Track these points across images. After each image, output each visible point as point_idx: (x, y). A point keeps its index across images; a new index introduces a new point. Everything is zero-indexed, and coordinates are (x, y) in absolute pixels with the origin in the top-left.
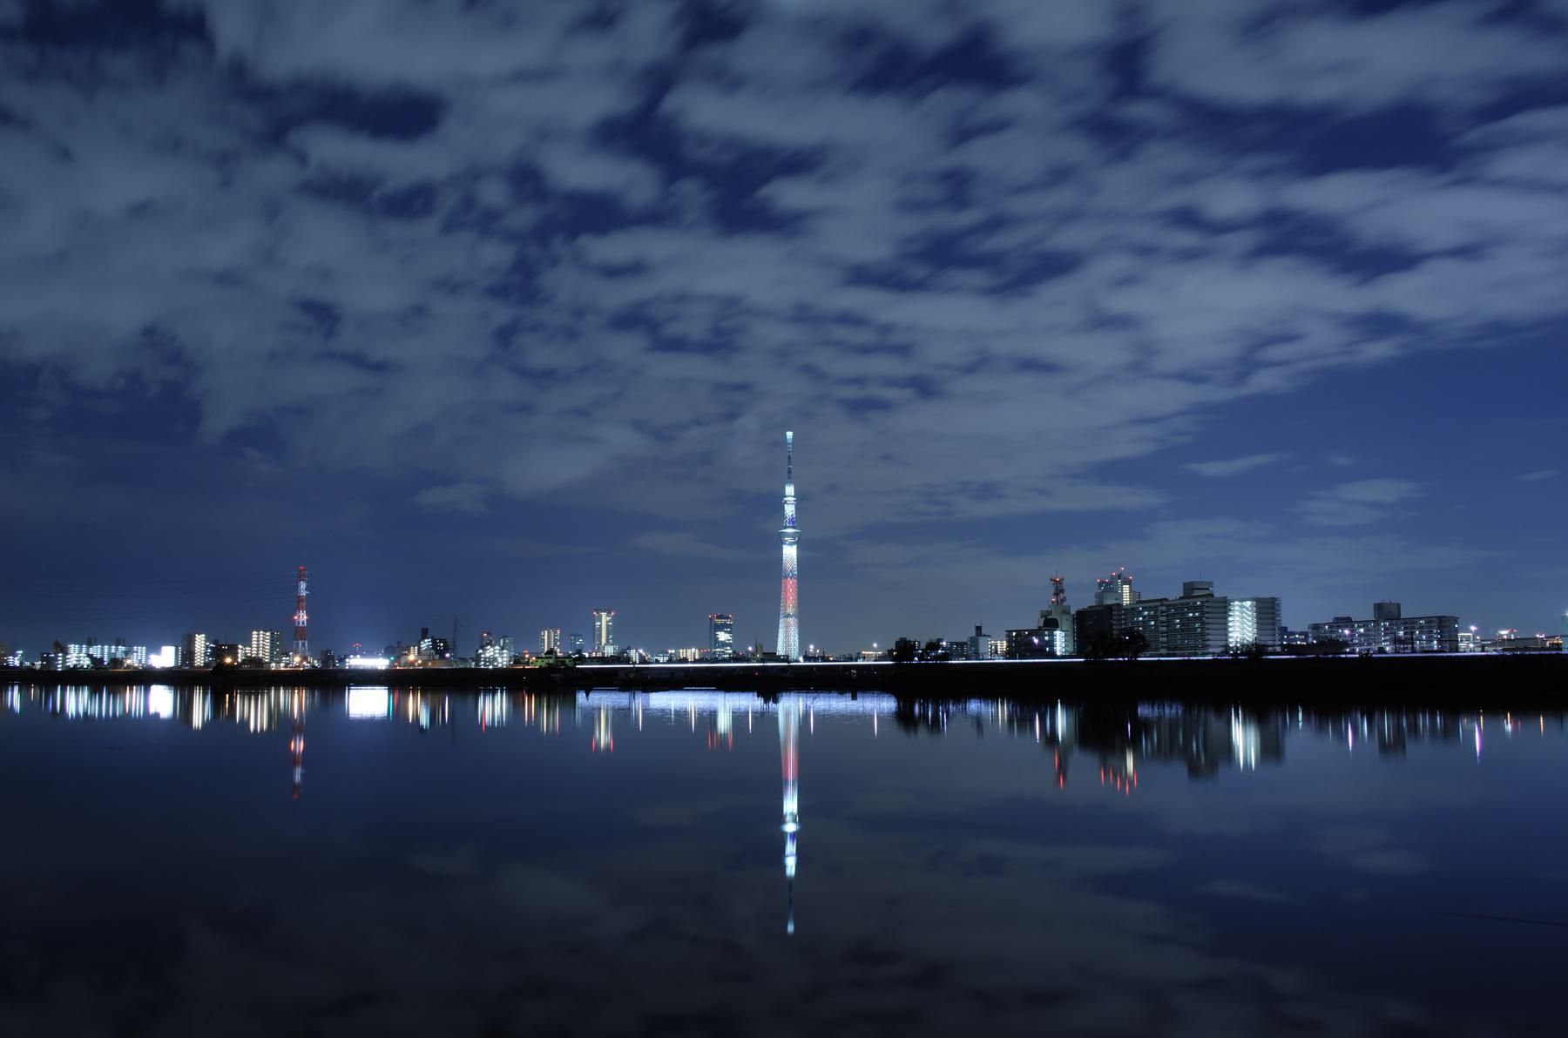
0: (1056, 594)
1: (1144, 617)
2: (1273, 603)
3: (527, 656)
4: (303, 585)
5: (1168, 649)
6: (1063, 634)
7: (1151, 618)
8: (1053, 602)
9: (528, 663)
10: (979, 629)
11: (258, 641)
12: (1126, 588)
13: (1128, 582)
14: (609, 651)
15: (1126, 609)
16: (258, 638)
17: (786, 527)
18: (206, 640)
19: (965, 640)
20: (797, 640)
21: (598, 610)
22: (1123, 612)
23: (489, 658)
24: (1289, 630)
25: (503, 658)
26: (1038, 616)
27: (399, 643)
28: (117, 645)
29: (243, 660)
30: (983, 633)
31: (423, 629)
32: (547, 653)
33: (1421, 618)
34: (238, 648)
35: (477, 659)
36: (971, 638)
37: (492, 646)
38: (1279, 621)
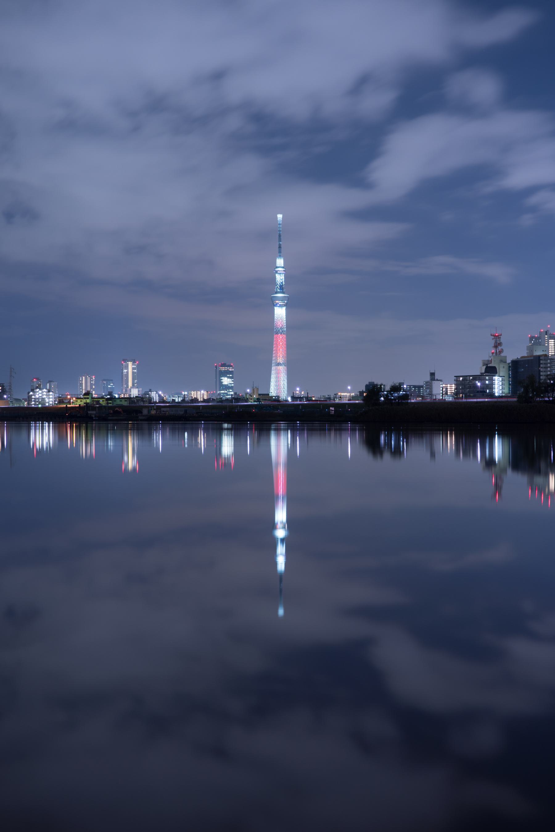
0: (496, 347)
3: (69, 397)
8: (493, 353)
9: (69, 403)
10: (432, 374)
14: (135, 393)
15: (551, 359)
17: (277, 293)
21: (125, 360)
22: (549, 361)
23: (38, 399)
25: (49, 398)
26: (481, 364)
30: (436, 378)
32: (85, 394)
35: (29, 399)
37: (40, 389)
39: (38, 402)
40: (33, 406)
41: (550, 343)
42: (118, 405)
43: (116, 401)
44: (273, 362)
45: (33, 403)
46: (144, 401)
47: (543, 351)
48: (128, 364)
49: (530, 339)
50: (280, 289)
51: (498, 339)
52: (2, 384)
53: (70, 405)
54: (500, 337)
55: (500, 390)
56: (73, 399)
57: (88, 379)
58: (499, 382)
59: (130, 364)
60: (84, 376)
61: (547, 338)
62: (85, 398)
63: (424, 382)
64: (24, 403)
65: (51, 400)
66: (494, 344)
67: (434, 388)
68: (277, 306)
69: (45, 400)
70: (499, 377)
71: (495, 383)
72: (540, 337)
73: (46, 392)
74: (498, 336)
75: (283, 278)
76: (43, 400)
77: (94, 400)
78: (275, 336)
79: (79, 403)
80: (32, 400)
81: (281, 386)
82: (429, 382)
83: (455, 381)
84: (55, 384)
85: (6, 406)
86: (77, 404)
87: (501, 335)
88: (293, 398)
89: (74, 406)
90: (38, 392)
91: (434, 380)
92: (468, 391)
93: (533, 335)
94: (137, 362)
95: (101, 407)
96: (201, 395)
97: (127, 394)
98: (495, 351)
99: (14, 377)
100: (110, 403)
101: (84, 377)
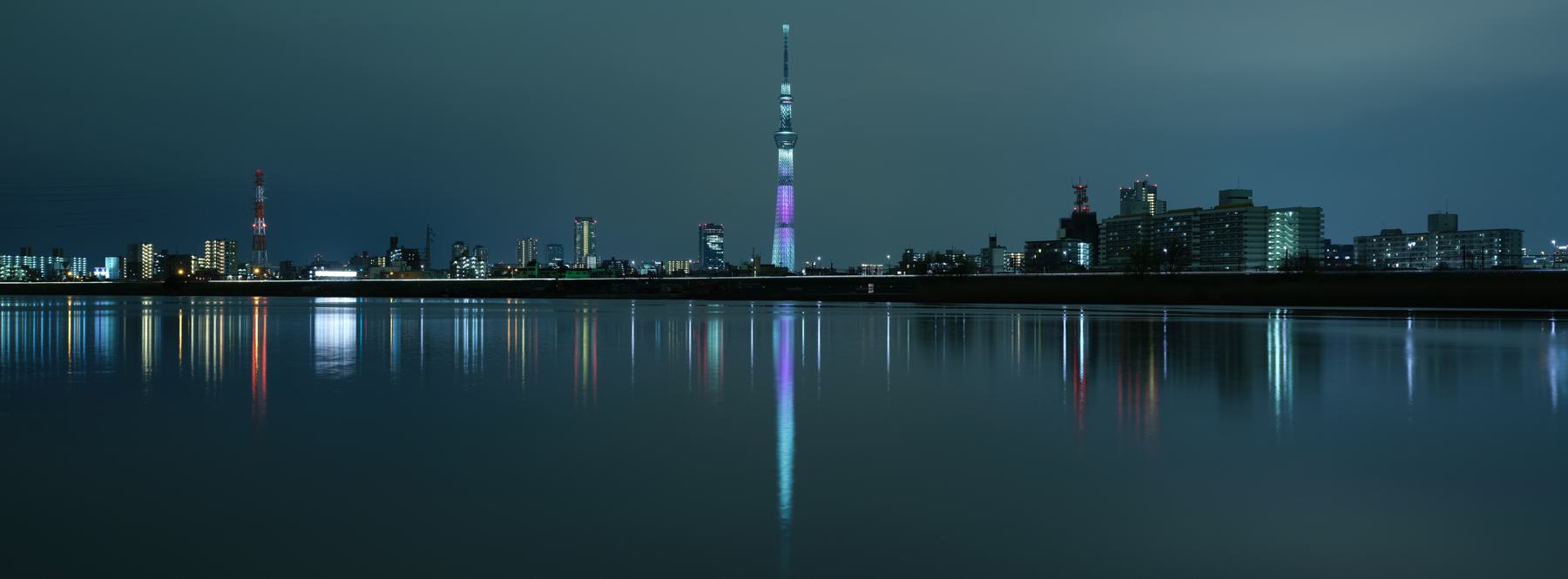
0: (1079, 203)
1: (1175, 228)
2: (1318, 213)
4: (261, 191)
5: (1201, 262)
7: (1184, 228)
10: (993, 240)
11: (211, 251)
12: (1151, 197)
13: (1153, 190)
16: (211, 248)
17: (781, 130)
18: (154, 251)
20: (793, 251)
24: (1332, 243)
25: (480, 269)
26: (1058, 225)
27: (365, 253)
28: (55, 256)
29: (196, 272)
31: (392, 238)
33: (1481, 231)
34: (191, 259)
36: (984, 250)
37: (468, 257)
38: (1323, 233)
50: (786, 125)
62: (530, 269)
88: (809, 271)
91: (996, 247)
96: (687, 265)
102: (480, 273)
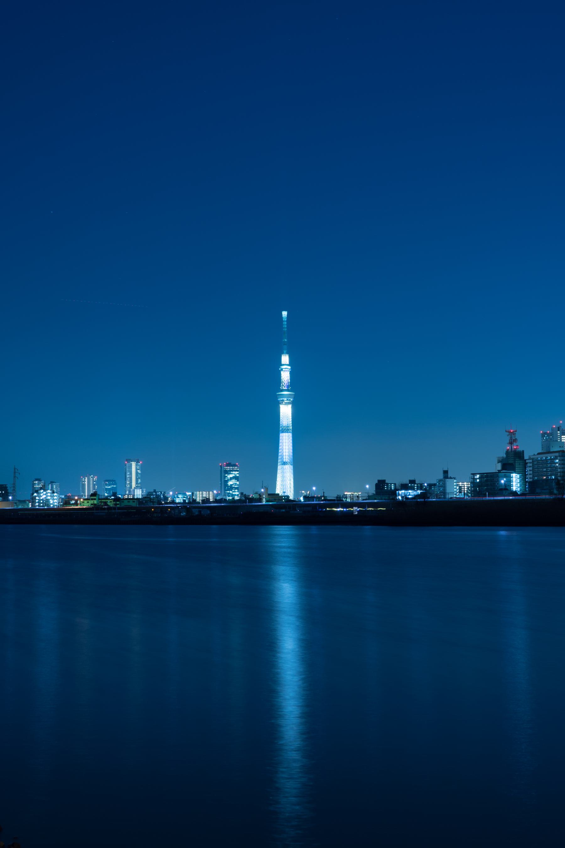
3: (76, 498)
6: (518, 476)
9: (76, 504)
10: (446, 472)
14: (139, 494)
17: (282, 390)
19: (435, 482)
21: (129, 460)
23: (42, 500)
25: (54, 499)
30: (449, 476)
32: (92, 495)
35: (33, 500)
36: (440, 481)
37: (45, 490)
39: (42, 503)
40: (37, 507)
41: (562, 439)
42: (127, 506)
43: (123, 502)
44: (279, 461)
45: (37, 504)
46: (153, 502)
47: (560, 447)
48: (131, 464)
49: (542, 435)
51: (513, 435)
52: (5, 485)
53: (77, 506)
54: (515, 433)
55: (518, 487)
56: (80, 500)
57: (91, 479)
58: (517, 479)
59: (134, 464)
60: (86, 476)
61: (559, 434)
62: (92, 499)
63: (437, 480)
64: (28, 504)
65: (55, 501)
66: (509, 441)
67: (447, 487)
68: (283, 404)
69: (50, 502)
70: (517, 474)
71: (512, 480)
72: (552, 433)
73: (50, 493)
74: (513, 432)
75: (289, 375)
76: (47, 501)
77: (102, 501)
78: (281, 435)
79: (86, 505)
80: (35, 502)
81: (287, 486)
82: (443, 480)
83: (471, 478)
84: (57, 485)
85: (10, 508)
86: (85, 505)
87: (516, 431)
89: (81, 507)
90: (42, 493)
91: (448, 478)
92: (486, 489)
93: (545, 431)
94: (141, 462)
95: (110, 508)
97: (131, 495)
98: (510, 448)
99: (18, 478)
100: (118, 504)
101: (86, 478)
102: (54, 503)
